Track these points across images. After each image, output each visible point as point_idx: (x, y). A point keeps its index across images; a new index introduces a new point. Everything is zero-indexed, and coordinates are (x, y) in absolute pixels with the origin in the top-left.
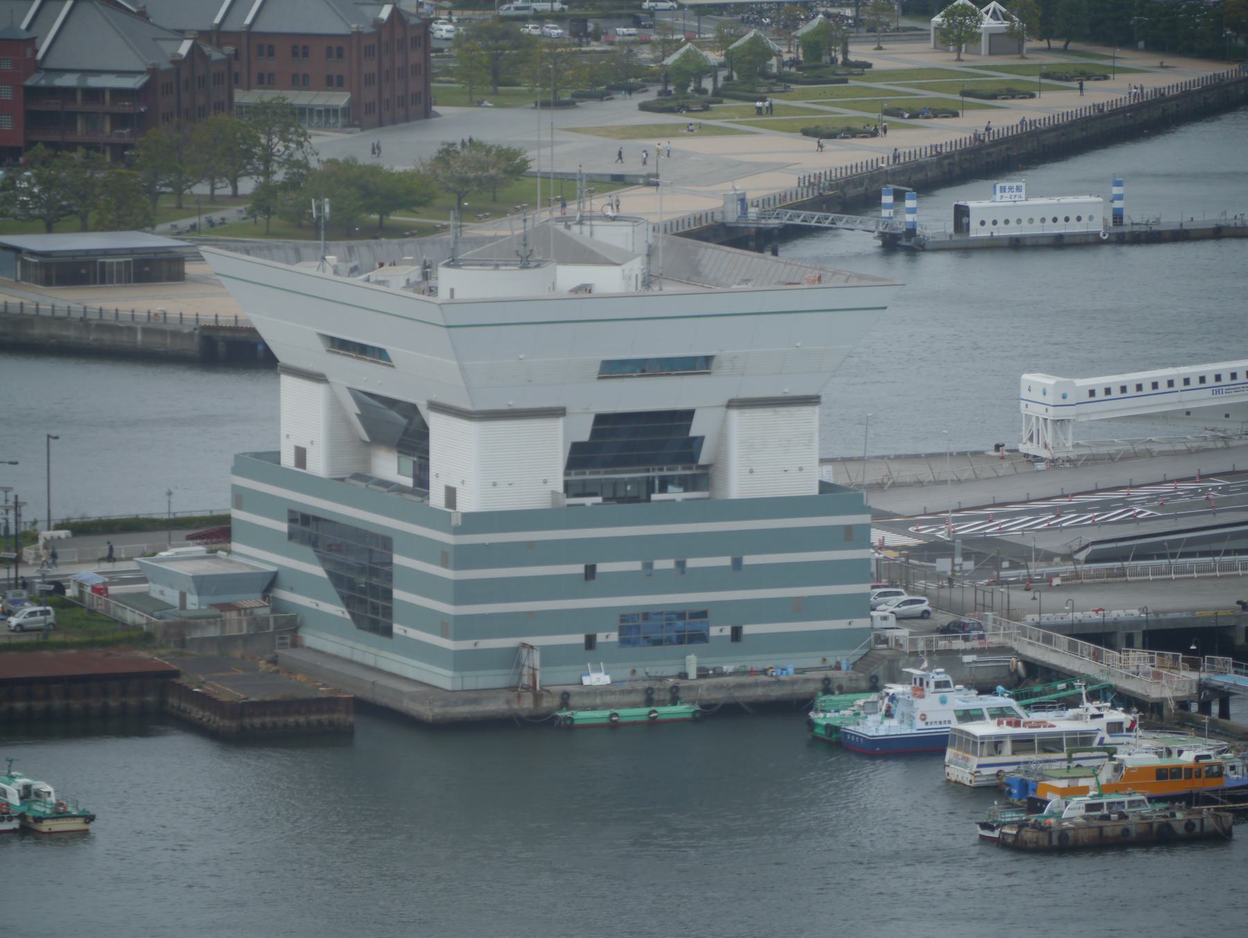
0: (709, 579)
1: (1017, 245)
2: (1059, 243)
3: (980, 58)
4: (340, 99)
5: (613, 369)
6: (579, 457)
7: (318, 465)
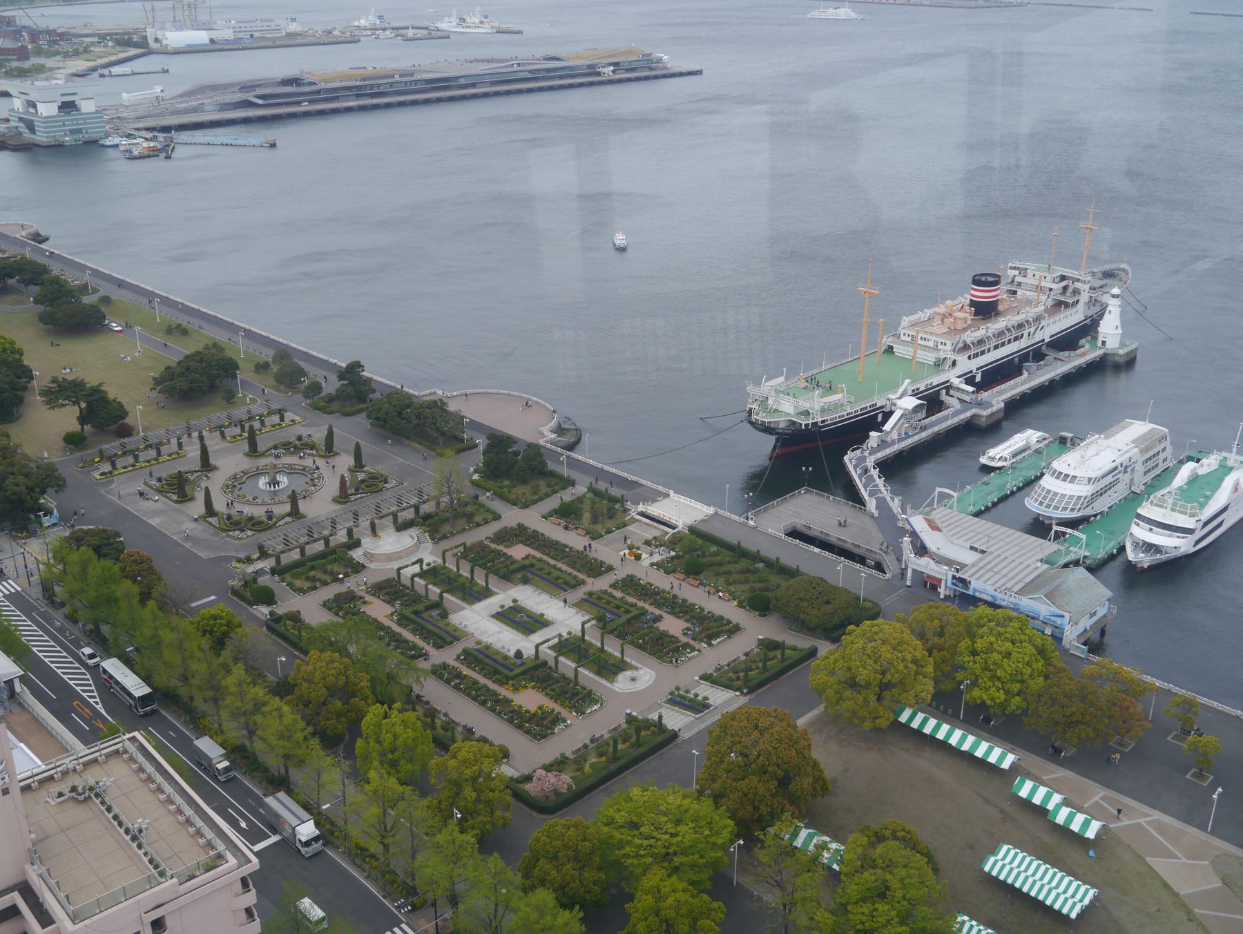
0: (81, 124)
1: (119, 75)
2: (125, 75)
3: (109, 49)
4: (16, 57)
5: (63, 95)
6: (60, 108)
7: (21, 110)
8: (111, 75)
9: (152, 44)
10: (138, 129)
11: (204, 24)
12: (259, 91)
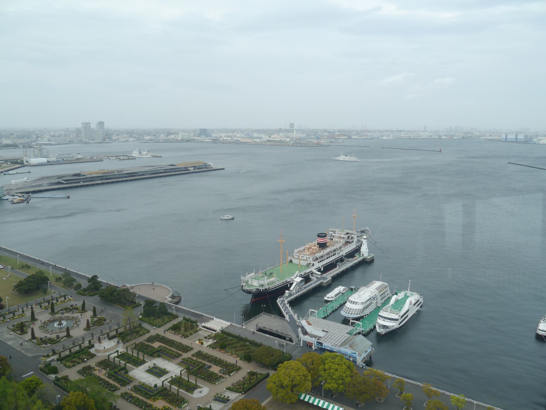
1: (11, 174)
8: (8, 174)
9: (25, 163)
10: (17, 193)
11: (45, 156)
12: (64, 179)
